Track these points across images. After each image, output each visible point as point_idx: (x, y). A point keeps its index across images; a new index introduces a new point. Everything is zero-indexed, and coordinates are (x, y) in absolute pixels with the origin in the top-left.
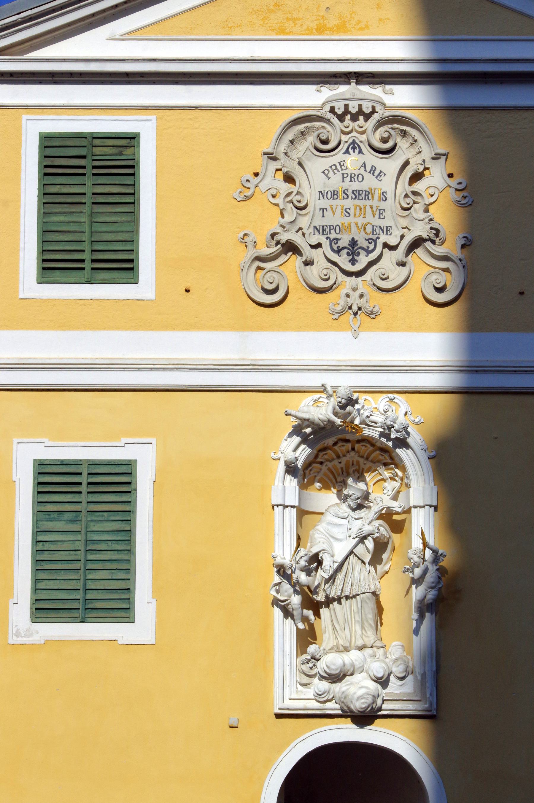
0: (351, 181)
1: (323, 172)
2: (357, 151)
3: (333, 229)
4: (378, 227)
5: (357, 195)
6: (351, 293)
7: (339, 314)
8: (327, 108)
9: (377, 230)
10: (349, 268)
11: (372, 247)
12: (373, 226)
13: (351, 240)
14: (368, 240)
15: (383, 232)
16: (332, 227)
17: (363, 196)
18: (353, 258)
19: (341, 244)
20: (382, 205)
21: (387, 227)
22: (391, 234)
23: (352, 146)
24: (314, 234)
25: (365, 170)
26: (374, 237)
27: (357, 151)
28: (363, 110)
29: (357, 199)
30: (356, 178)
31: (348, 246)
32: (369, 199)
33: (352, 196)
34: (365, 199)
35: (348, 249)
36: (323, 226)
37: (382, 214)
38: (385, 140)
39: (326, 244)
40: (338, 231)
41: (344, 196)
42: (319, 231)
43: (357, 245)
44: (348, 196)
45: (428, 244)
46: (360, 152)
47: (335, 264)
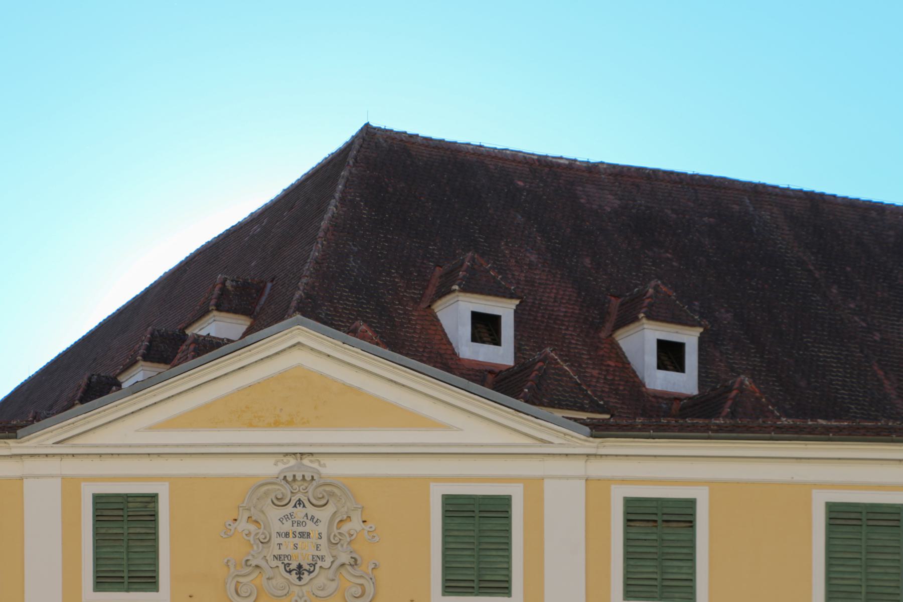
0: (298, 526)
1: (280, 520)
2: (302, 506)
5: (302, 535)
11: (312, 569)
12: (313, 556)
14: (309, 565)
15: (319, 559)
17: (306, 535)
18: (300, 576)
19: (292, 567)
20: (319, 542)
21: (322, 556)
23: (298, 502)
25: (307, 519)
26: (314, 563)
27: (302, 506)
30: (301, 524)
36: (280, 555)
39: (282, 567)
40: (289, 559)
42: (277, 559)
44: (296, 536)
45: (349, 568)
46: (304, 506)
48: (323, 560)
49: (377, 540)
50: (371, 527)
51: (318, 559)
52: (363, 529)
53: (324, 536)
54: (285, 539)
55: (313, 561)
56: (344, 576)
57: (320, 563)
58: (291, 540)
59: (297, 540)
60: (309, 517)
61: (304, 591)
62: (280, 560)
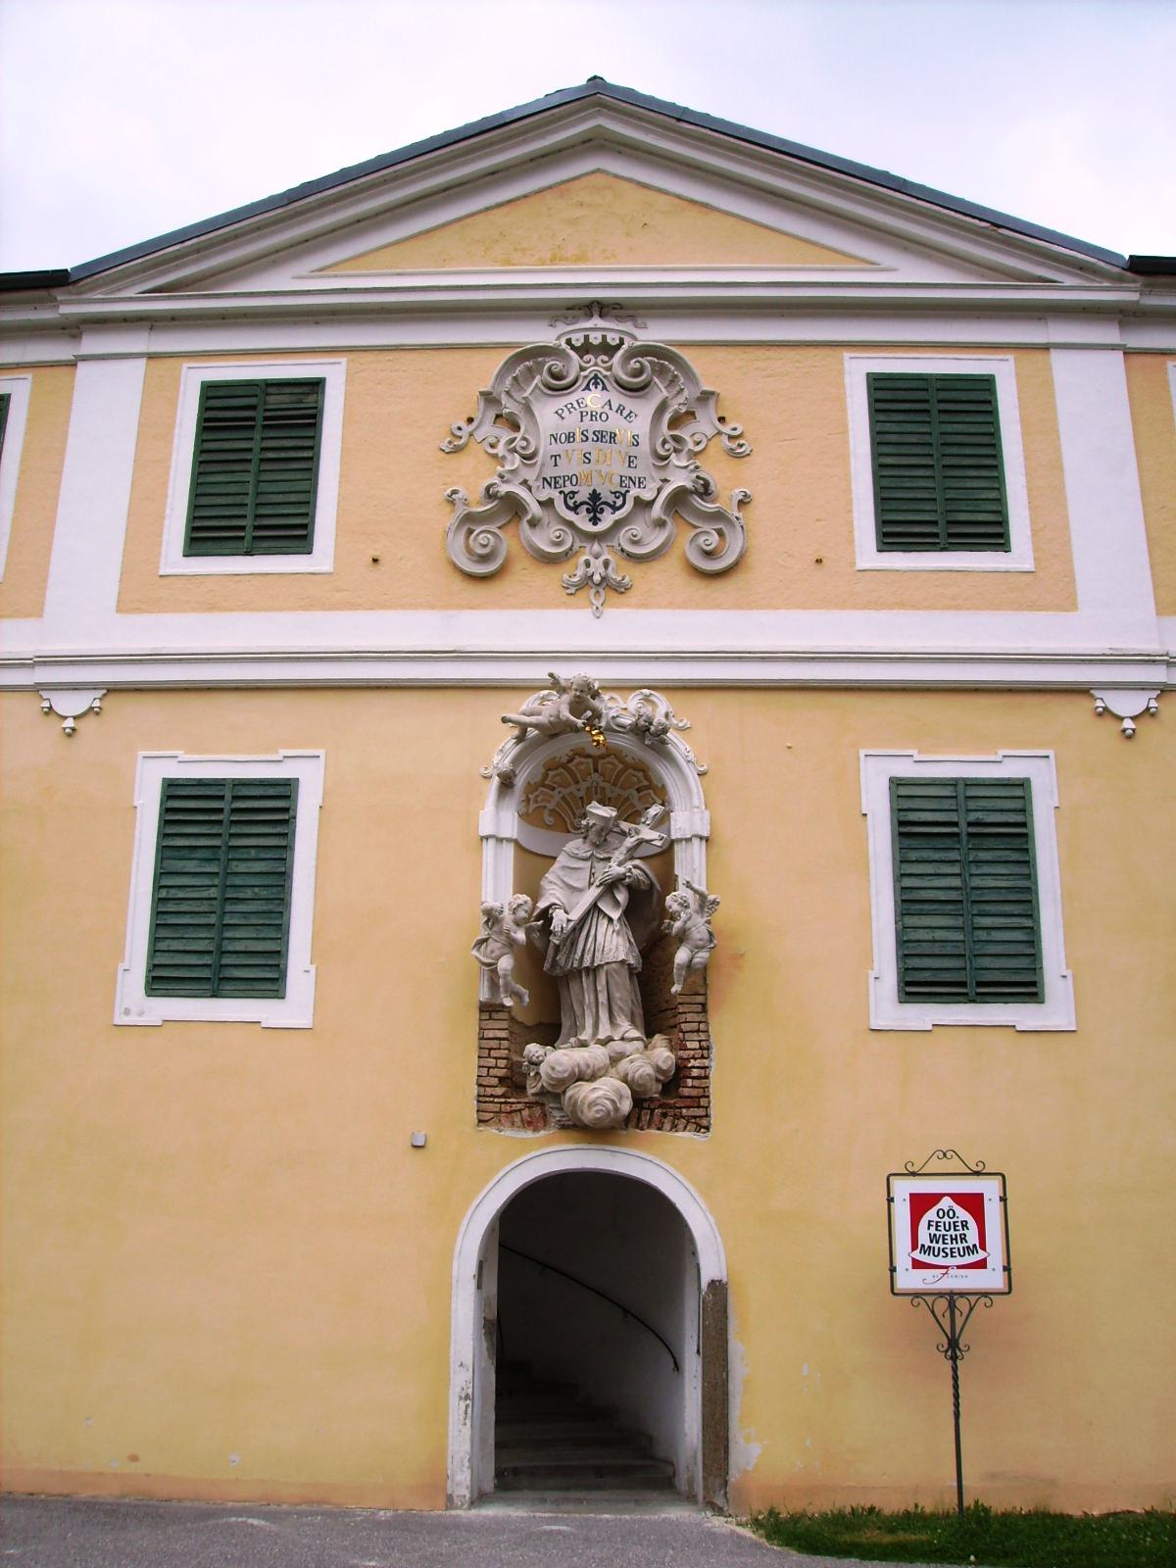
0: (592, 420)
1: (556, 412)
2: (600, 387)
6: (592, 560)
10: (589, 528)
11: (619, 502)
12: (621, 477)
14: (615, 493)
15: (634, 483)
17: (608, 438)
18: (595, 516)
19: (579, 498)
20: (633, 451)
25: (611, 409)
26: (623, 490)
27: (600, 387)
30: (598, 416)
35: (588, 504)
36: (555, 478)
38: (638, 373)
40: (574, 483)
42: (550, 485)
44: (587, 438)
48: (642, 486)
50: (735, 429)
52: (719, 433)
53: (644, 441)
54: (567, 446)
55: (621, 486)
57: (634, 492)
58: (579, 446)
59: (588, 446)
60: (615, 408)
62: (555, 487)
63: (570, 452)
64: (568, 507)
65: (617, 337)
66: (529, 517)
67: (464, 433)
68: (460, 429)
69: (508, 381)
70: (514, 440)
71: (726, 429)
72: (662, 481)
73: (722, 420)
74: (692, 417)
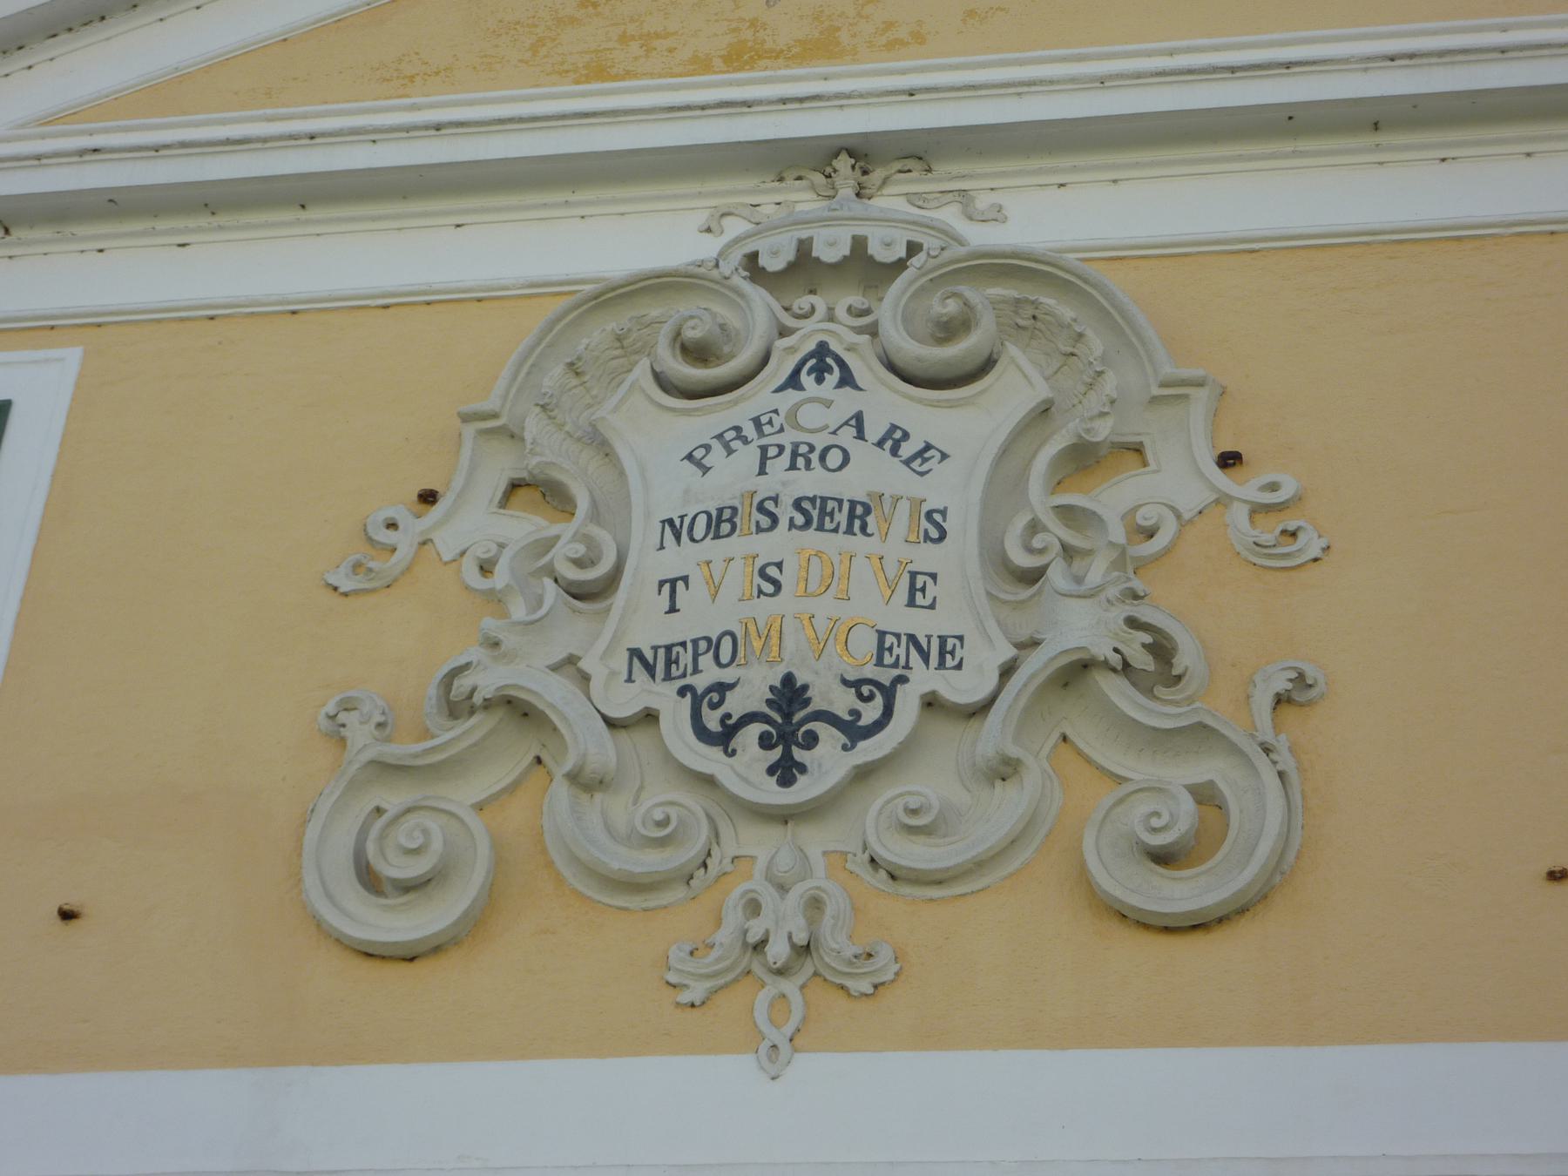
0: (793, 467)
1: (690, 457)
2: (832, 378)
3: (708, 650)
4: (904, 639)
5: (815, 514)
6: (768, 896)
7: (709, 984)
8: (737, 256)
9: (900, 651)
10: (771, 793)
11: (871, 712)
12: (882, 635)
13: (777, 684)
14: (856, 685)
15: (925, 657)
16: (703, 645)
17: (842, 518)
18: (787, 755)
19: (736, 704)
20: (926, 557)
21: (943, 640)
22: (959, 667)
23: (812, 362)
24: (630, 680)
25: (860, 435)
26: (886, 677)
27: (832, 378)
28: (870, 251)
29: (811, 530)
30: (815, 457)
31: (767, 710)
32: (869, 531)
33: (791, 519)
34: (850, 531)
35: (766, 719)
36: (669, 648)
37: (923, 590)
38: (948, 330)
39: (675, 714)
40: (725, 656)
41: (758, 522)
42: (650, 669)
43: (807, 702)
45: (1115, 689)
46: (847, 380)
47: (709, 781)
48: (949, 662)
49: (1315, 552)
51: (914, 656)
52: (1223, 500)
55: (880, 662)
56: (1080, 753)
57: (923, 679)
59: (778, 544)
60: (874, 431)
61: (815, 853)
63: (718, 567)
64: (702, 732)
65: (901, 238)
66: (568, 765)
67: (404, 541)
68: (392, 525)
69: (554, 375)
70: (549, 544)
71: (1245, 487)
72: (1021, 646)
73: (1229, 460)
74: (1132, 457)
